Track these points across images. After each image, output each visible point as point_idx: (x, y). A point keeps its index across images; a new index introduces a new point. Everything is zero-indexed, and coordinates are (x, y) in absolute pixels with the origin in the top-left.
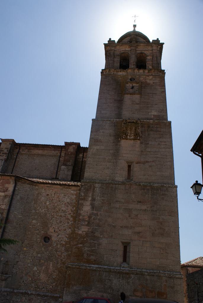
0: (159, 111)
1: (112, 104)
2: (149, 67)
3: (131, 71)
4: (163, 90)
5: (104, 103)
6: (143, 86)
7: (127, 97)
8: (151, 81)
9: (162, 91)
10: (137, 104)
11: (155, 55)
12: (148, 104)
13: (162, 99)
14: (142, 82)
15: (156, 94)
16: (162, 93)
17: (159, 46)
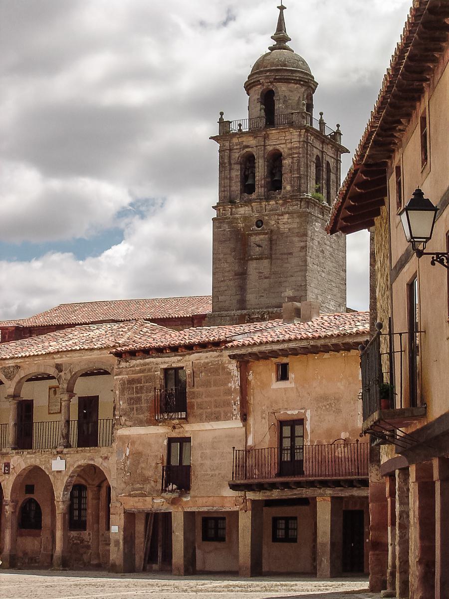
0: (294, 289)
1: (232, 282)
2: (285, 188)
3: (257, 205)
4: (302, 244)
5: (222, 281)
6: (274, 237)
7: (252, 266)
8: (286, 226)
9: (301, 247)
10: (266, 278)
11: (296, 155)
12: (280, 277)
13: (300, 263)
14: (272, 231)
15: (291, 254)
16: (300, 251)
17: (302, 131)
